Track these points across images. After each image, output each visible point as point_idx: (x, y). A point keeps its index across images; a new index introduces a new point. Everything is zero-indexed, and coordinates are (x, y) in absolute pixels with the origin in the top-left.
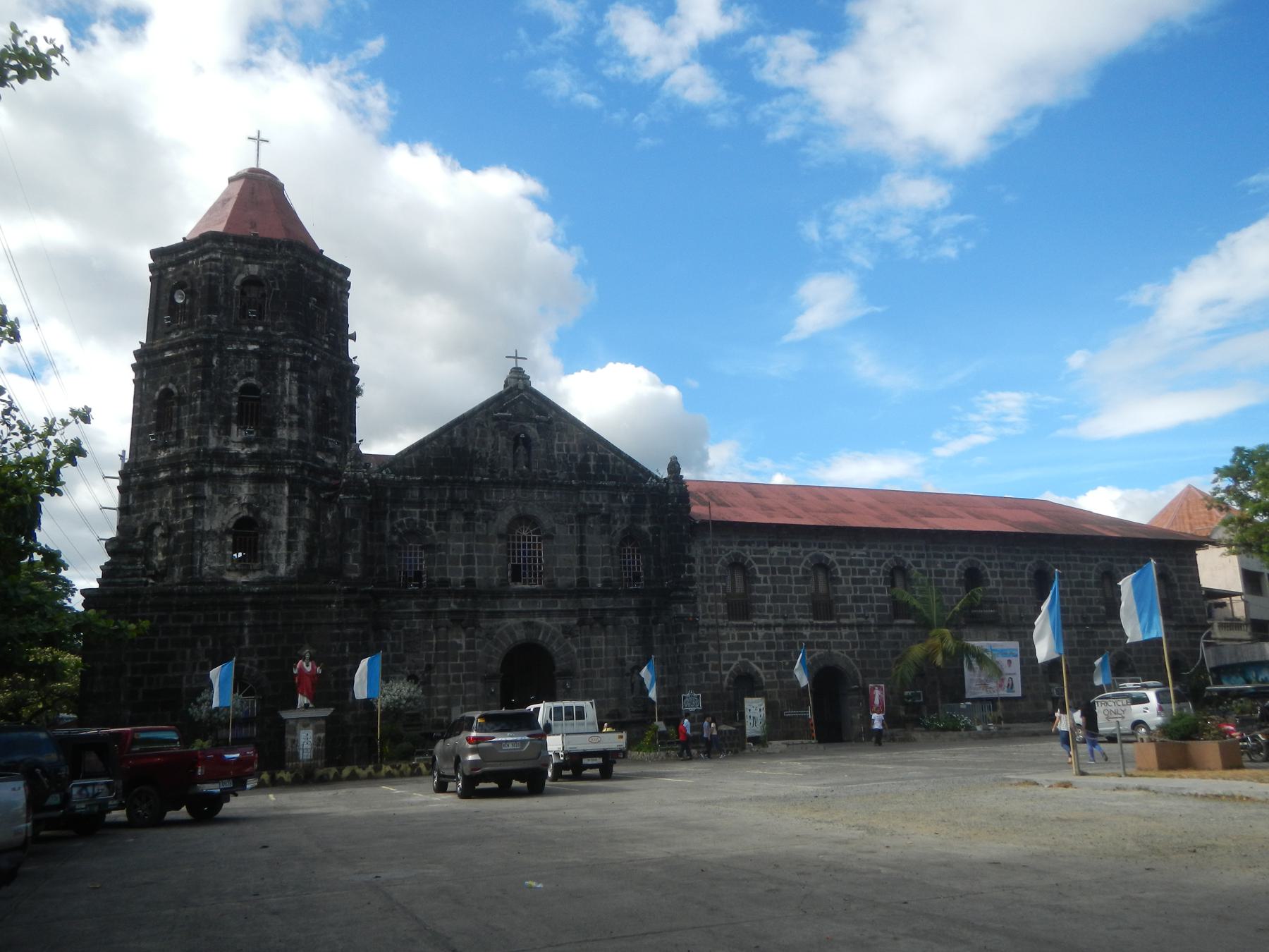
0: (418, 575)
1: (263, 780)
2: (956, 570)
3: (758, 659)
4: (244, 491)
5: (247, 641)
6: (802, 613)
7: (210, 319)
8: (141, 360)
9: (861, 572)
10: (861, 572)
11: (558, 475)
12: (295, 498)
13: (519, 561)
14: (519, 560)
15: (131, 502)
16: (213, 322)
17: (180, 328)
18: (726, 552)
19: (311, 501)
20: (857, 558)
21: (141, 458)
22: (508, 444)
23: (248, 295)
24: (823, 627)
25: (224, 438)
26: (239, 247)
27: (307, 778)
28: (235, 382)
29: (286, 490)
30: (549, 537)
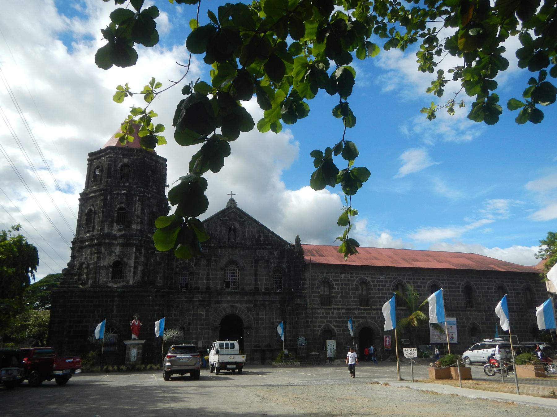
0: (187, 285)
1: (115, 369)
2: (427, 285)
3: (334, 323)
4: (117, 250)
5: (115, 311)
6: (355, 304)
7: (107, 181)
8: (82, 197)
9: (382, 286)
10: (382, 286)
11: (247, 244)
12: (138, 253)
13: (230, 279)
14: (230, 279)
15: (75, 253)
16: (109, 182)
17: (96, 184)
18: (321, 276)
19: (144, 254)
20: (381, 279)
21: (81, 236)
22: (226, 230)
23: (124, 171)
24: (364, 309)
25: (111, 228)
26: (121, 152)
27: (133, 369)
28: (116, 206)
29: (134, 249)
30: (243, 269)
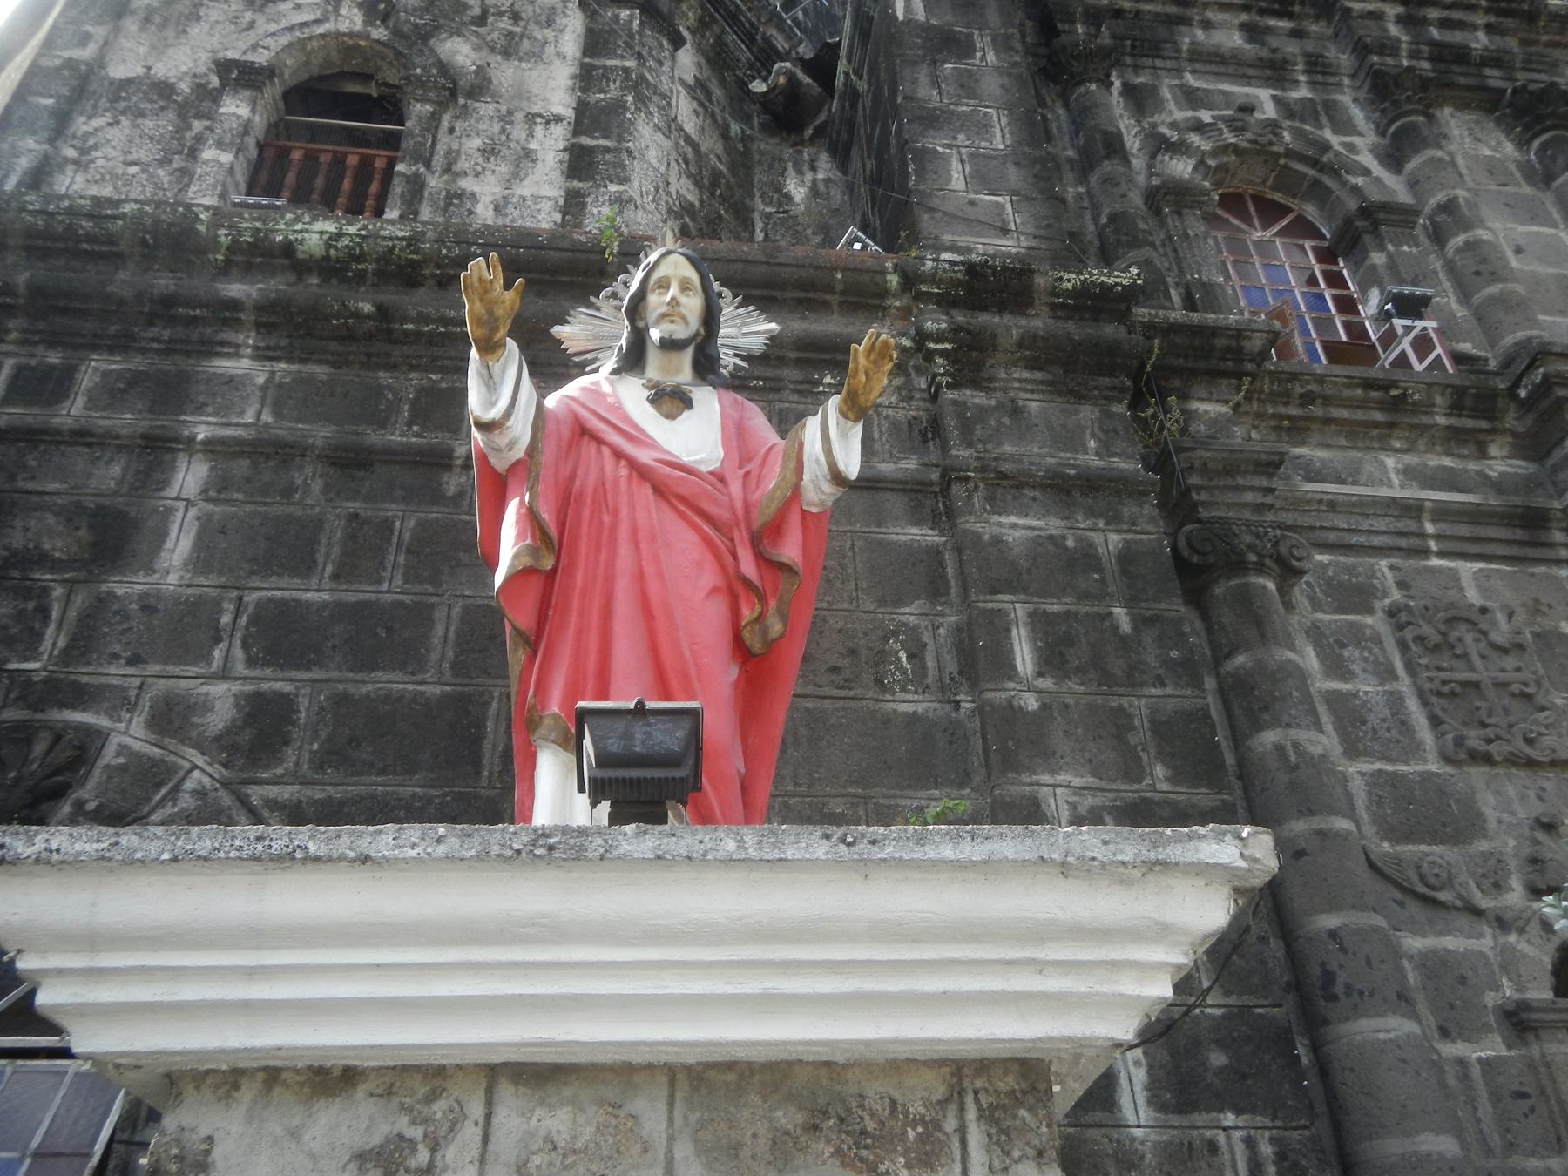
5: (179, 546)
